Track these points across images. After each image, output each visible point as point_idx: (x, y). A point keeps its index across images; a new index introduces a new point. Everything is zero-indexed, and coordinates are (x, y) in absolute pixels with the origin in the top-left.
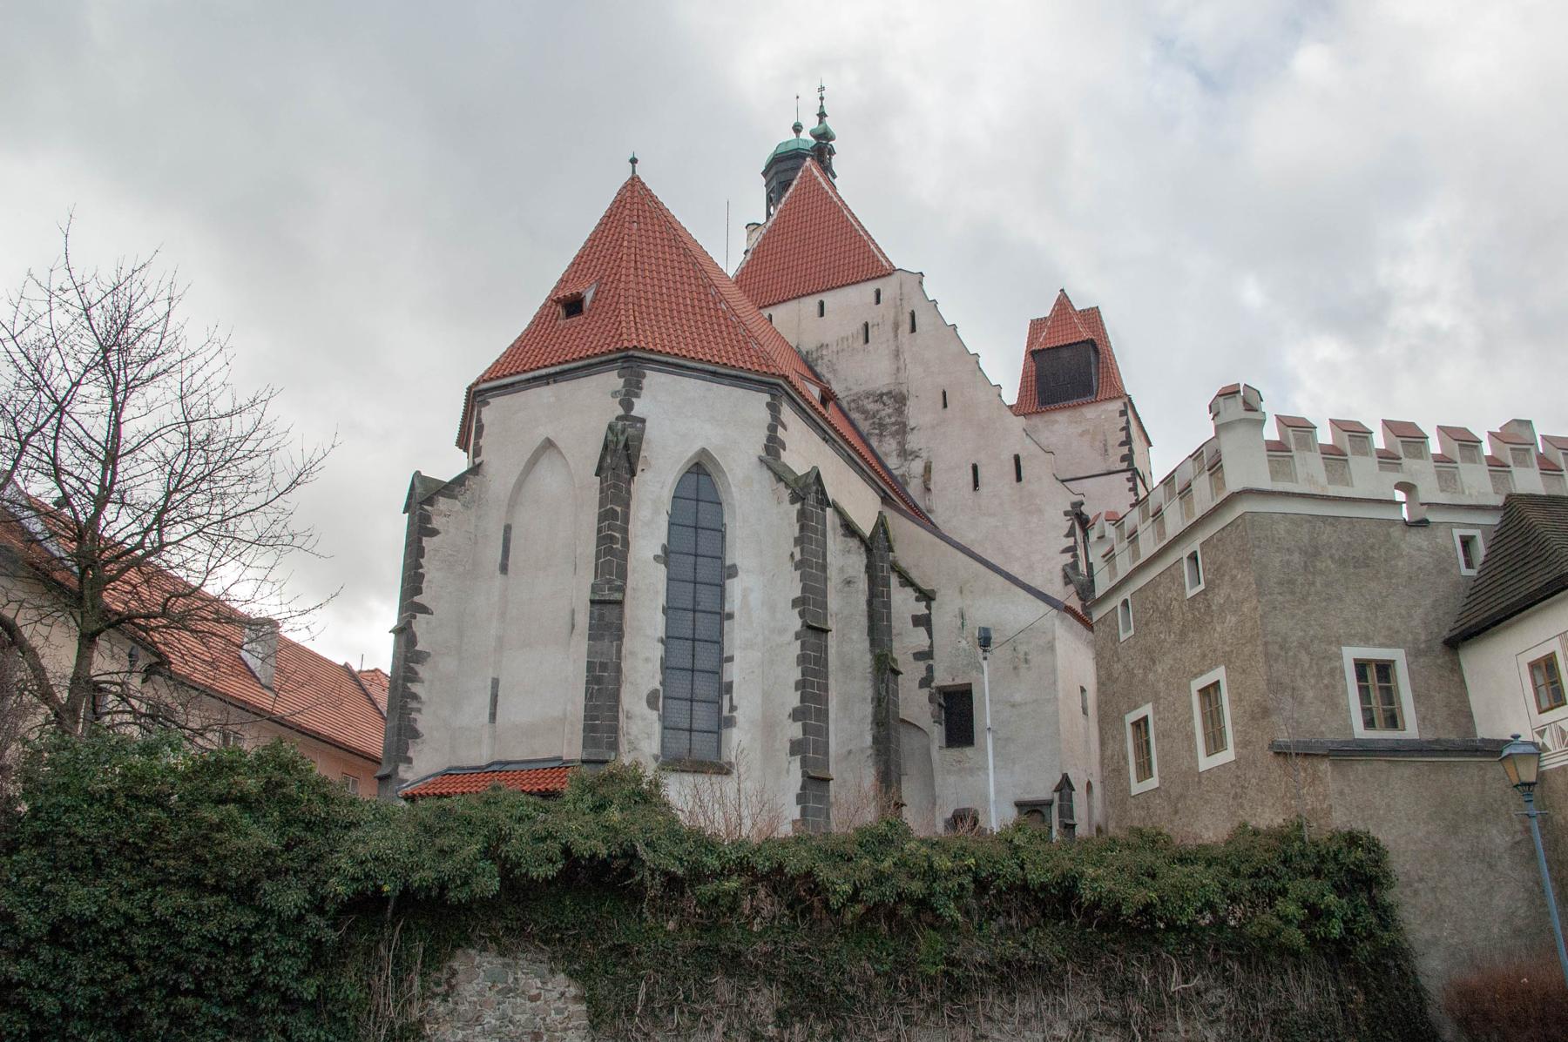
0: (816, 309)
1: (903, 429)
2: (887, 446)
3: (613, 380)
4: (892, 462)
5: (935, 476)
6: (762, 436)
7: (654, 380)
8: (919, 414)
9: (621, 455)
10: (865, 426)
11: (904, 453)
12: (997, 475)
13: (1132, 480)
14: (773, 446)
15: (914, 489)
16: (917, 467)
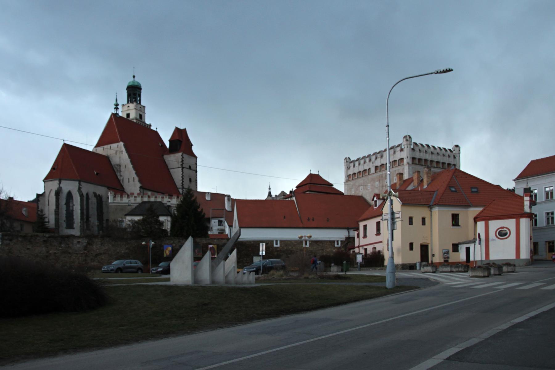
0: (109, 147)
1: (120, 171)
2: (118, 174)
3: (57, 182)
4: (119, 177)
5: (124, 180)
6: (77, 188)
7: (63, 182)
8: (123, 169)
9: (58, 193)
10: (116, 170)
11: (121, 176)
12: (131, 180)
13: (182, 169)
14: (79, 189)
15: (121, 182)
16: (122, 178)
